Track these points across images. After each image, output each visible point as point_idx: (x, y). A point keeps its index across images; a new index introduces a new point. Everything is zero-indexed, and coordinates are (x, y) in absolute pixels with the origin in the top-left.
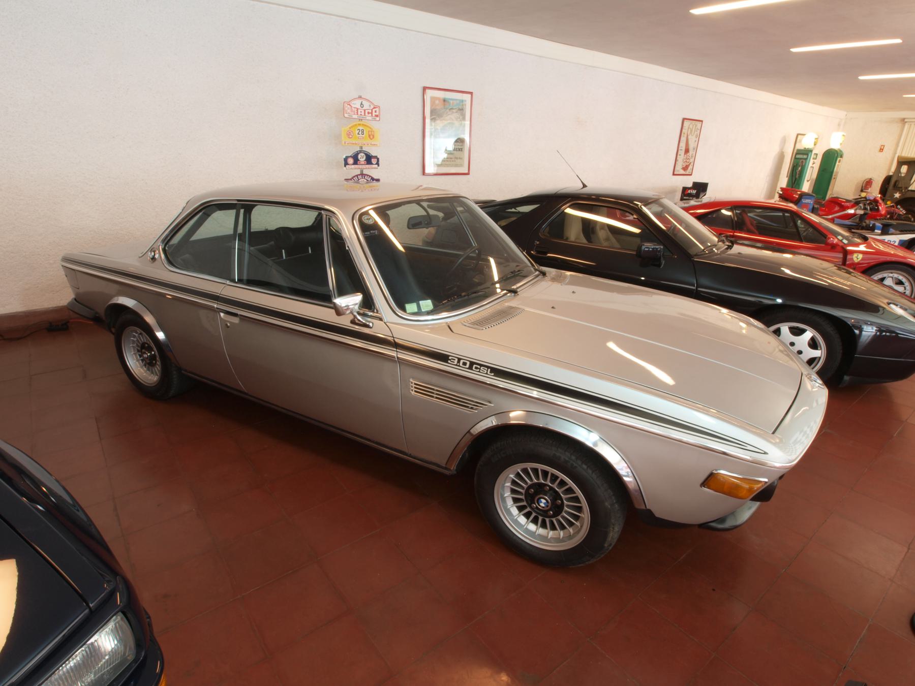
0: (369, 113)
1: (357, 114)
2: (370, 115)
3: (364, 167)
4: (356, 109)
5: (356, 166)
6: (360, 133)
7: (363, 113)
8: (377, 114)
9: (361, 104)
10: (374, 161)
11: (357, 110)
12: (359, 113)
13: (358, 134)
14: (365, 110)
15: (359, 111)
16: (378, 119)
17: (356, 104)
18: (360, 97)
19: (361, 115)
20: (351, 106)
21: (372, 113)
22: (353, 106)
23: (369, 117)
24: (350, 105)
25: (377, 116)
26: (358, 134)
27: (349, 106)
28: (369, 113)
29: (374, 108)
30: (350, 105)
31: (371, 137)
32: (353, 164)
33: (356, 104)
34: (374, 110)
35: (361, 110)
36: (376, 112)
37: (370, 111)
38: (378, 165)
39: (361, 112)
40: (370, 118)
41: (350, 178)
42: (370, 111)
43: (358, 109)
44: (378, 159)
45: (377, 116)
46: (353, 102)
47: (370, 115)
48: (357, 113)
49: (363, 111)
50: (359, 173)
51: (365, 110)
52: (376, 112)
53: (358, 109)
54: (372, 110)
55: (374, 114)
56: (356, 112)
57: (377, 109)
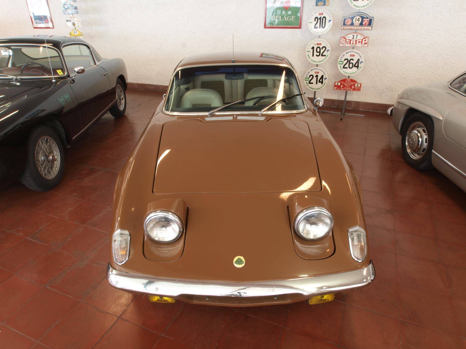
0: (359, 42)
1: (350, 43)
4: (349, 40)
7: (354, 43)
8: (366, 42)
11: (350, 41)
12: (352, 43)
14: (356, 41)
15: (352, 41)
16: (366, 45)
17: (350, 37)
19: (353, 44)
20: (346, 39)
21: (362, 42)
22: (347, 38)
23: (359, 45)
24: (345, 38)
25: (366, 43)
27: (344, 39)
28: (359, 42)
29: (364, 38)
30: (345, 38)
33: (350, 37)
34: (364, 40)
35: (353, 41)
36: (365, 41)
39: (353, 42)
40: (360, 45)
42: (361, 41)
43: (350, 40)
45: (366, 43)
46: (347, 36)
49: (355, 41)
51: (356, 41)
52: (365, 41)
53: (350, 40)
54: (362, 40)
55: (364, 42)
56: (349, 42)
57: (367, 39)
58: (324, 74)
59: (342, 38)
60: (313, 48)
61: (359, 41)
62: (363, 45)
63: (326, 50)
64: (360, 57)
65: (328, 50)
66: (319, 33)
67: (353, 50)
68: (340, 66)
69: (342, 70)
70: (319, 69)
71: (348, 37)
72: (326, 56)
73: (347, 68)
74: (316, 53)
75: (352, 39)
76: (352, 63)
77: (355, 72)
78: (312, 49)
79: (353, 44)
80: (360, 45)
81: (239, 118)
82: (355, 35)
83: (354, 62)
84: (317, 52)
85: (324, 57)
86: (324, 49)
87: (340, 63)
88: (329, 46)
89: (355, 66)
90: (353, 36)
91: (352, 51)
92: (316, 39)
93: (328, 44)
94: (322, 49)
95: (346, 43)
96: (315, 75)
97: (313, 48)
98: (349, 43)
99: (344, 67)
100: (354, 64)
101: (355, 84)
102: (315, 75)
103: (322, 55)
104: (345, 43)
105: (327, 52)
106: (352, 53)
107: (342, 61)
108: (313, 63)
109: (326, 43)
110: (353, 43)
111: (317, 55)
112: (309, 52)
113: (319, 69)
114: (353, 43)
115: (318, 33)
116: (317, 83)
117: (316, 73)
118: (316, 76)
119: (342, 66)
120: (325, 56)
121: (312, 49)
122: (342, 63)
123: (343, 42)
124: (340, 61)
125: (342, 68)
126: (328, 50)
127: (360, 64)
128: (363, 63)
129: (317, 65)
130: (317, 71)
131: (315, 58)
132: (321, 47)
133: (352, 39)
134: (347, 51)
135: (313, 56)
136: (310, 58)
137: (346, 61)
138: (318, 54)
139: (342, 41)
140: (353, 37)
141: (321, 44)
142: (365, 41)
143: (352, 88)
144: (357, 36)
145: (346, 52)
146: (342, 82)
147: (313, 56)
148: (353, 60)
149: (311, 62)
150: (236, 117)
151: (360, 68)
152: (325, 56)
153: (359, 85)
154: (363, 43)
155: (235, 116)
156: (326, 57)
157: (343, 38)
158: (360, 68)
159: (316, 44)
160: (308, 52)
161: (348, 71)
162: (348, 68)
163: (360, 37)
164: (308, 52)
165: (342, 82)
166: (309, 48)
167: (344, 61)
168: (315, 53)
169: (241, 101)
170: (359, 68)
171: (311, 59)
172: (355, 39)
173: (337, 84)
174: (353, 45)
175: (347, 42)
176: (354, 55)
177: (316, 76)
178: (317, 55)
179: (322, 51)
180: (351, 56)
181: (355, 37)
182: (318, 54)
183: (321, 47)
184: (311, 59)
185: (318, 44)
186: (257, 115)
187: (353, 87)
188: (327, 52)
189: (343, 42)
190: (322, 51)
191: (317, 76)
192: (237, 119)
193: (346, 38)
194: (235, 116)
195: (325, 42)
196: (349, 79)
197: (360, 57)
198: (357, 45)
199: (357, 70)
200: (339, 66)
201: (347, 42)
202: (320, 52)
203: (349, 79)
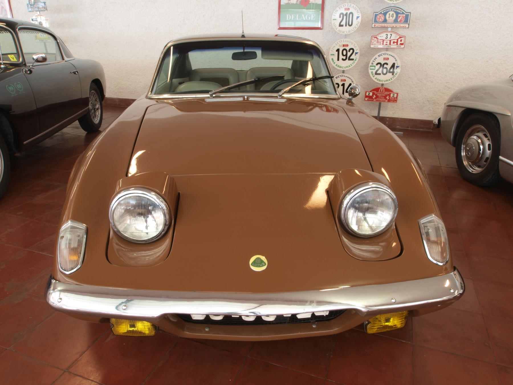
0: (394, 42)
1: (383, 44)
2: (395, 44)
4: (382, 41)
7: (388, 43)
8: (402, 42)
12: (385, 43)
14: (390, 41)
15: (385, 41)
16: (402, 46)
17: (383, 36)
19: (386, 44)
20: (378, 39)
21: (397, 42)
22: (379, 38)
23: (394, 46)
24: (376, 38)
27: (375, 39)
28: (394, 42)
29: (400, 38)
30: (376, 38)
33: (383, 36)
34: (399, 40)
35: (387, 41)
36: (401, 41)
37: (396, 41)
39: (387, 42)
40: (395, 46)
42: (396, 41)
43: (383, 40)
45: (402, 44)
47: (395, 44)
49: (389, 42)
51: (390, 41)
52: (401, 41)
53: (383, 40)
54: (398, 40)
55: (399, 42)
56: (382, 42)
57: (403, 39)
58: (352, 82)
59: (373, 38)
60: (338, 50)
61: (394, 41)
62: (399, 47)
63: (354, 53)
64: (396, 60)
65: (356, 53)
66: (345, 32)
67: (387, 52)
68: (372, 72)
69: (374, 76)
70: (346, 77)
71: (381, 37)
72: (354, 59)
73: (380, 74)
74: (342, 56)
75: (386, 38)
76: (386, 68)
77: (390, 79)
78: (337, 52)
79: (386, 44)
80: (395, 46)
81: (251, 99)
82: (389, 34)
83: (389, 67)
84: (343, 55)
85: (351, 62)
86: (351, 51)
87: (371, 68)
88: (357, 48)
89: (390, 72)
90: (386, 35)
91: (386, 54)
92: (342, 40)
93: (356, 45)
94: (349, 51)
95: (378, 44)
96: (341, 84)
97: (338, 50)
98: (381, 44)
99: (376, 74)
100: (388, 69)
101: (390, 94)
102: (341, 84)
103: (349, 59)
104: (377, 44)
105: (355, 55)
106: (386, 56)
107: (374, 65)
108: (338, 68)
109: (353, 44)
110: (386, 43)
111: (343, 59)
112: (334, 55)
113: (346, 77)
114: (386, 43)
115: (344, 32)
116: (343, 93)
117: (342, 80)
118: (342, 85)
119: (374, 72)
120: (353, 59)
121: (337, 52)
122: (373, 68)
123: (375, 42)
124: (371, 66)
125: (374, 75)
126: (356, 53)
127: (396, 68)
128: (399, 67)
129: (343, 72)
130: (343, 78)
131: (341, 63)
132: (348, 49)
133: (386, 38)
134: (380, 54)
135: (338, 60)
136: (334, 63)
137: (379, 65)
138: (344, 58)
139: (373, 41)
140: (387, 36)
141: (347, 45)
142: (400, 42)
143: (386, 99)
144: (391, 35)
145: (378, 54)
146: (374, 92)
147: (338, 60)
148: (387, 64)
149: (336, 67)
150: (248, 98)
151: (395, 74)
152: (353, 59)
153: (395, 96)
154: (399, 44)
155: (246, 97)
156: (354, 61)
157: (375, 37)
158: (395, 74)
159: (342, 46)
160: (331, 55)
161: (382, 77)
162: (382, 74)
163: (394, 37)
164: (331, 55)
165: (374, 92)
166: (333, 50)
167: (376, 66)
168: (341, 57)
169: (253, 80)
170: (394, 74)
171: (336, 64)
172: (388, 39)
173: (368, 95)
174: (386, 47)
175: (379, 43)
176: (388, 59)
177: (342, 85)
178: (343, 59)
179: (349, 54)
180: (384, 59)
181: (389, 36)
182: (344, 58)
183: (348, 49)
184: (336, 64)
185: (344, 46)
186: (276, 97)
187: (388, 97)
188: (355, 55)
190: (349, 54)
191: (343, 85)
192: (249, 100)
193: (378, 37)
194: (246, 97)
195: (352, 44)
196: (382, 88)
197: (396, 60)
198: (392, 47)
199: (393, 76)
200: (370, 71)
201: (379, 43)
202: (346, 55)
203: (382, 88)
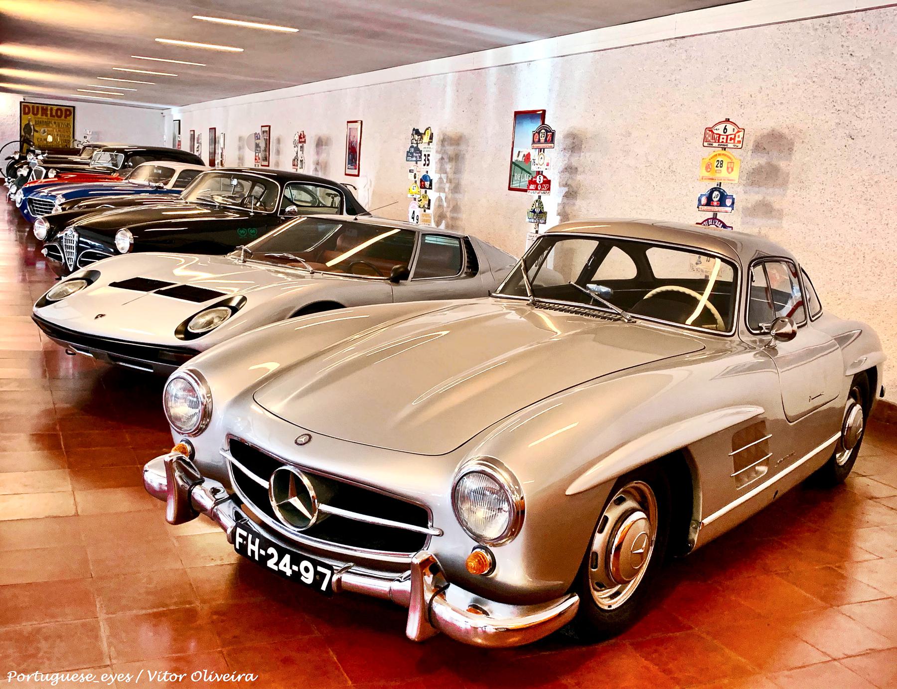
0: (731, 139)
1: (719, 142)
2: (732, 141)
3: (716, 209)
4: (718, 136)
5: (709, 208)
6: (719, 165)
7: (725, 141)
8: (740, 139)
9: (725, 129)
10: (728, 202)
11: (719, 137)
12: (721, 140)
13: (717, 167)
14: (727, 136)
15: (721, 137)
16: (740, 146)
18: (728, 120)
19: (723, 142)
22: (715, 132)
26: (717, 167)
27: (710, 133)
28: (731, 140)
29: (738, 132)
31: (730, 170)
32: (706, 205)
34: (737, 135)
37: (733, 136)
38: (733, 209)
41: (701, 222)
44: (733, 199)
46: (715, 128)
48: (719, 140)
49: (725, 137)
50: (712, 217)
52: (739, 137)
56: (717, 139)
59: (708, 131)
71: (716, 129)
98: (717, 141)
114: (723, 140)
154: (736, 142)
157: (709, 130)
189: (709, 138)
